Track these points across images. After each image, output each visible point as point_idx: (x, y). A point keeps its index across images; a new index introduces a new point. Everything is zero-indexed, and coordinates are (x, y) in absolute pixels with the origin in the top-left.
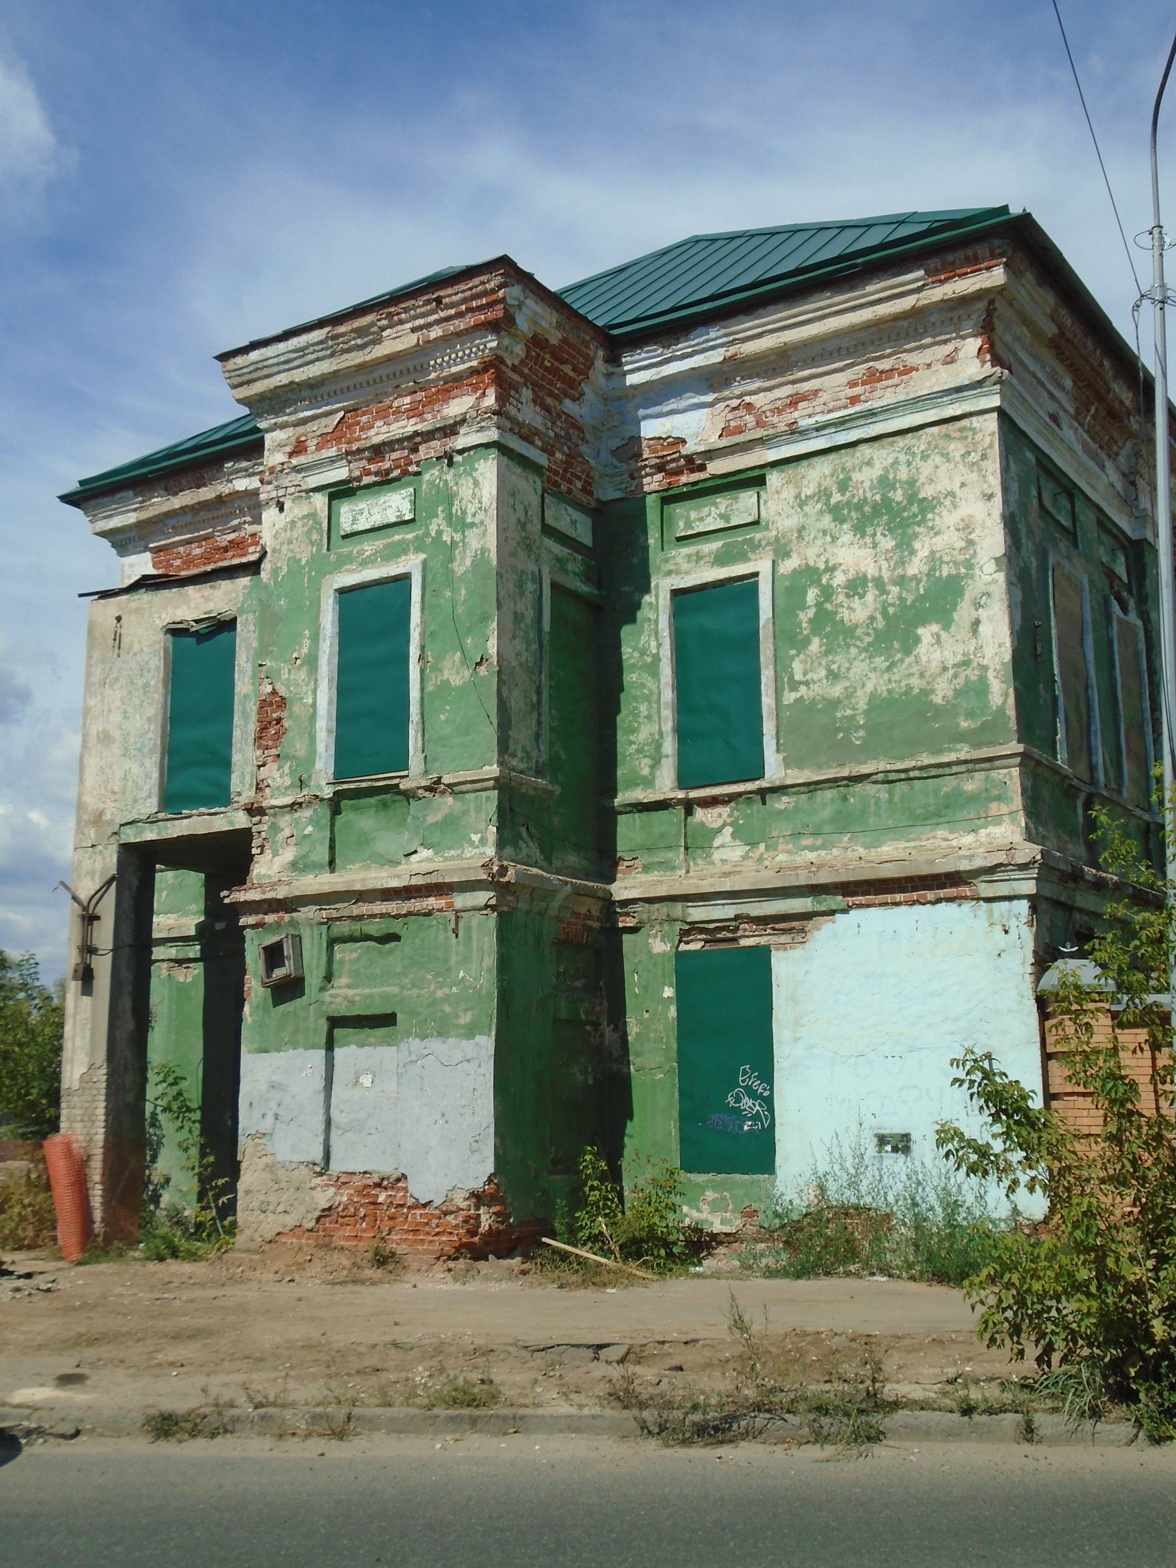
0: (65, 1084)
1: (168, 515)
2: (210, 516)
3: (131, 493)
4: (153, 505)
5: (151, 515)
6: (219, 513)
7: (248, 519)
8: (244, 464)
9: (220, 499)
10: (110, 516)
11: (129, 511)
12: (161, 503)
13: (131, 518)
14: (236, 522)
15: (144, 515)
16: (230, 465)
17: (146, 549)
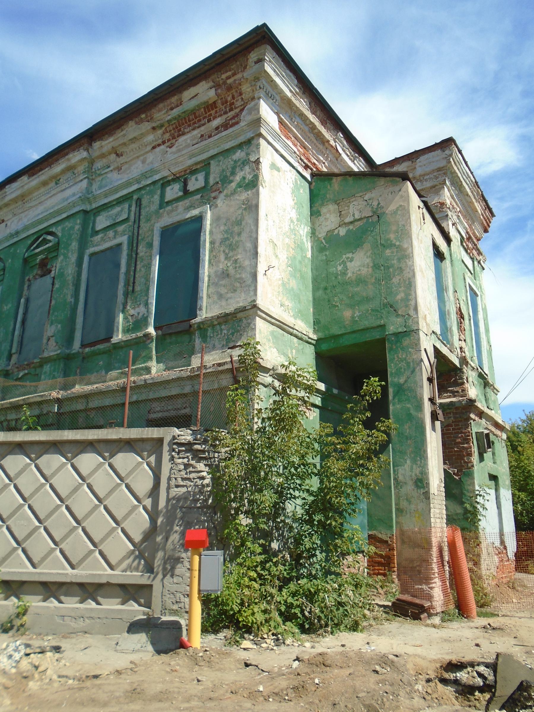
0: (432, 491)
1: (302, 115)
2: (315, 141)
3: (296, 82)
4: (300, 101)
5: (298, 106)
6: (318, 144)
7: (326, 164)
8: (345, 143)
9: (324, 142)
10: (278, 75)
11: (288, 87)
12: (302, 104)
13: (289, 94)
14: (322, 159)
15: (293, 99)
16: (342, 135)
17: (277, 114)
